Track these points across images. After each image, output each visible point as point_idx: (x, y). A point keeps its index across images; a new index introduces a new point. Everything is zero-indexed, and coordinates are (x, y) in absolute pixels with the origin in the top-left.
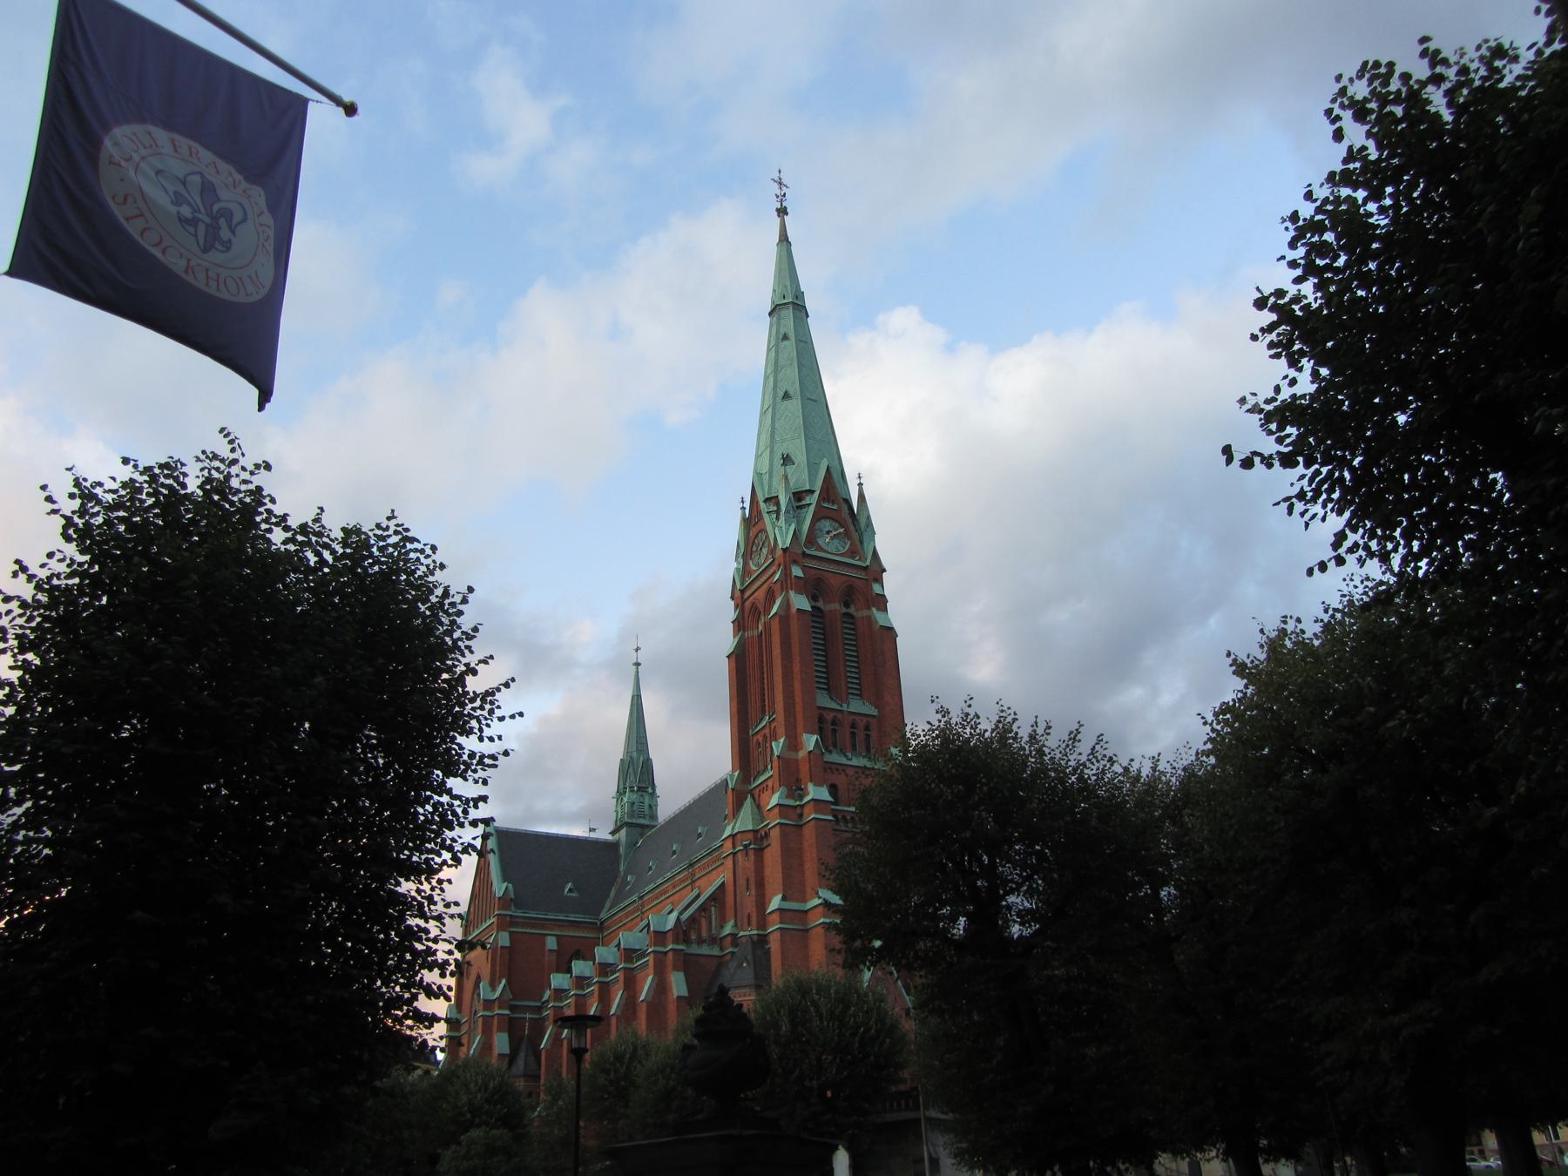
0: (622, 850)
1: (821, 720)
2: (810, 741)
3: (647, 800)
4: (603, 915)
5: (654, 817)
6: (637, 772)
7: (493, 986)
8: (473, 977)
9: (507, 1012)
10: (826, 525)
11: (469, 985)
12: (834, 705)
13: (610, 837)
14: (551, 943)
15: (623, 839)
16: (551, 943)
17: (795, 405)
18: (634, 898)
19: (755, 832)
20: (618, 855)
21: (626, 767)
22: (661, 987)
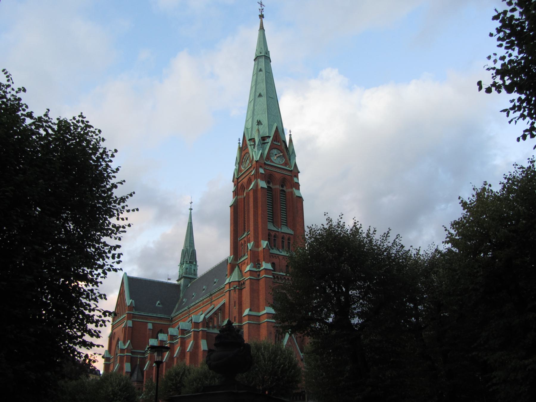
0: (181, 288)
1: (269, 235)
2: (264, 244)
3: (193, 267)
4: (172, 315)
5: (195, 274)
6: (189, 256)
7: (125, 343)
8: (116, 339)
9: (130, 354)
10: (275, 151)
11: (114, 342)
12: (275, 229)
13: (176, 282)
14: (150, 326)
15: (182, 284)
16: (150, 326)
17: (264, 99)
18: (186, 308)
19: (239, 282)
20: (179, 291)
21: (185, 253)
22: (196, 346)
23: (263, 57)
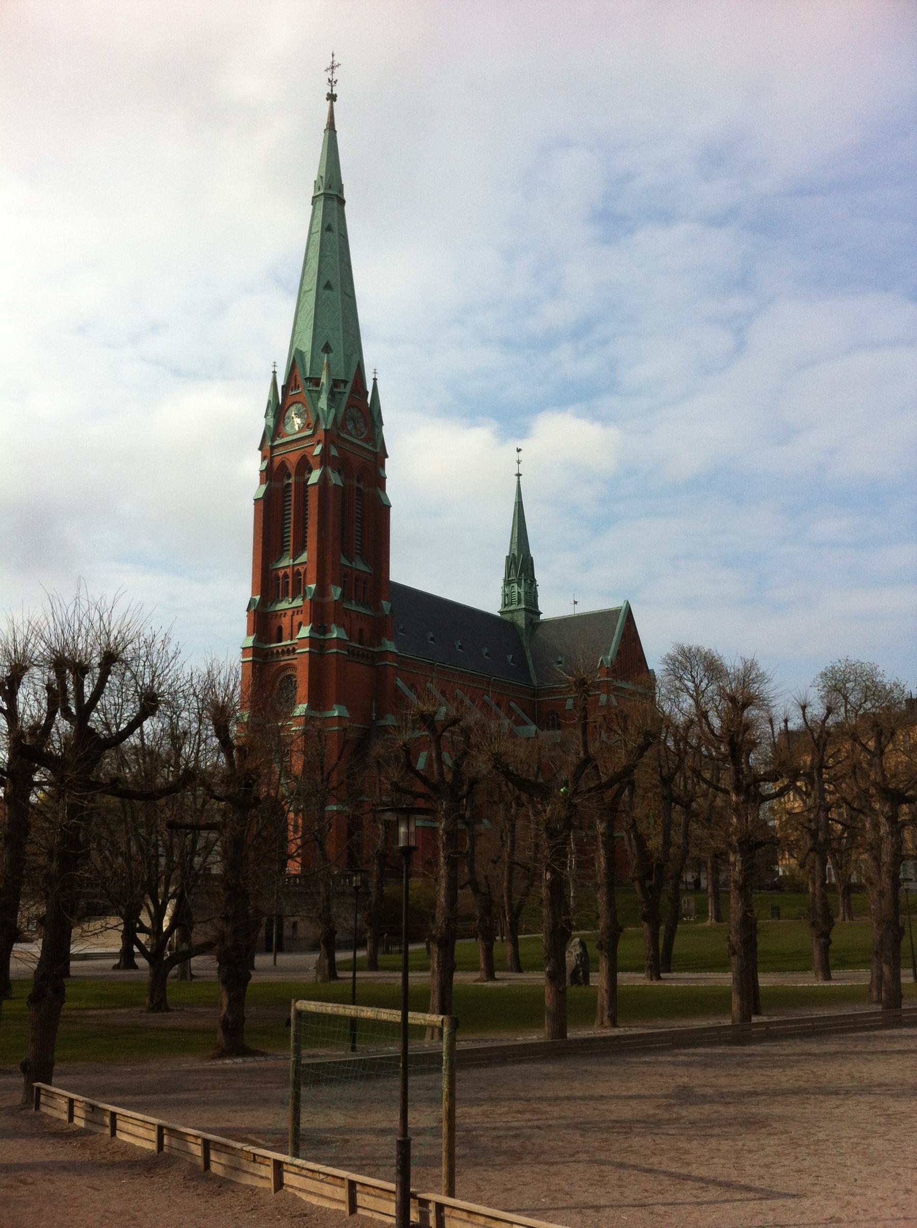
2: (336, 593)
12: (348, 564)
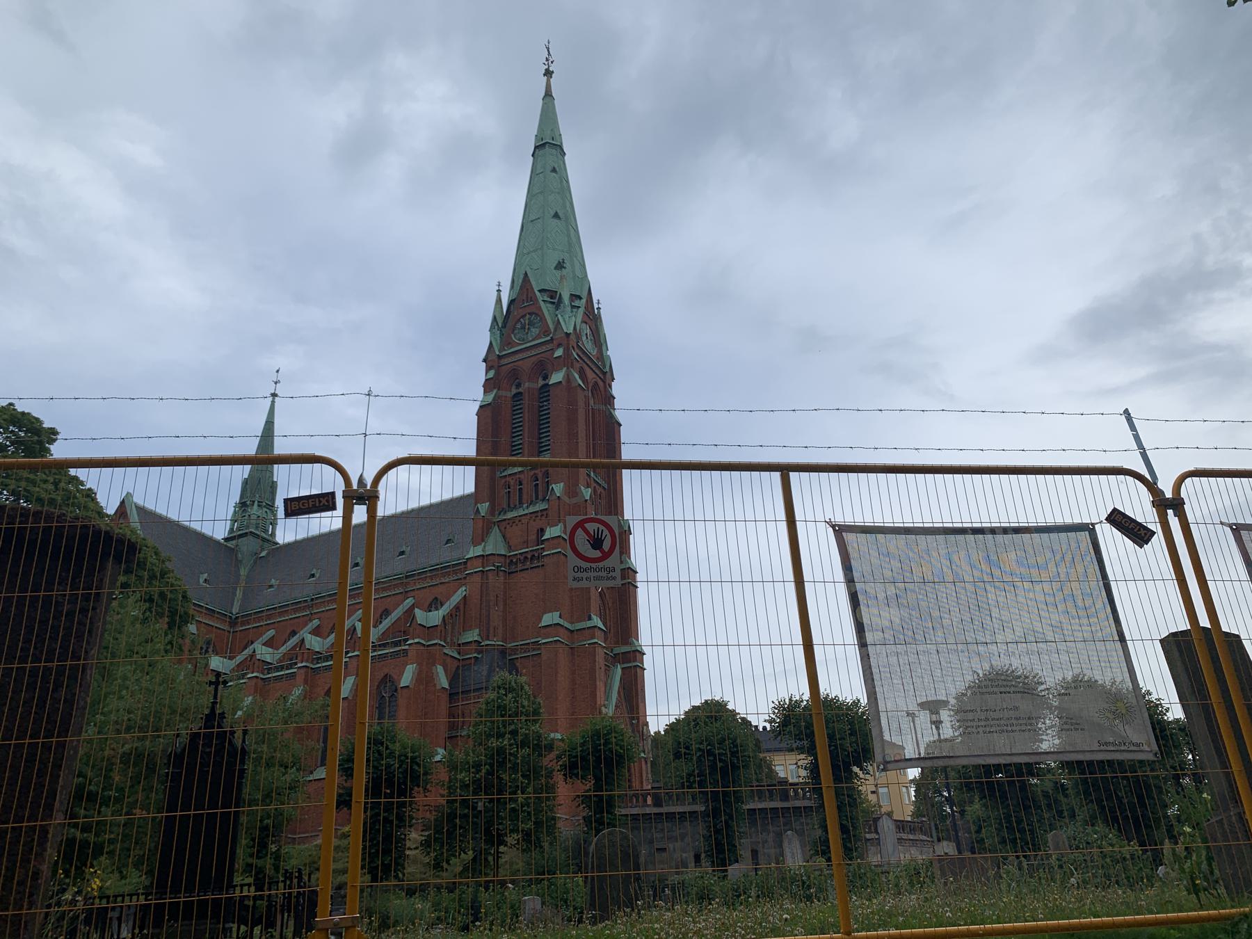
20: (238, 563)
23: (548, 147)
